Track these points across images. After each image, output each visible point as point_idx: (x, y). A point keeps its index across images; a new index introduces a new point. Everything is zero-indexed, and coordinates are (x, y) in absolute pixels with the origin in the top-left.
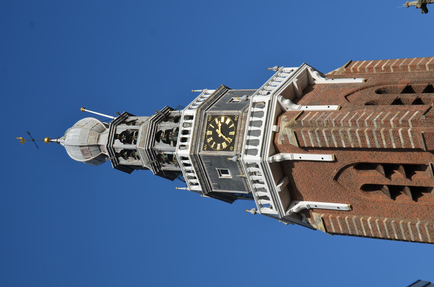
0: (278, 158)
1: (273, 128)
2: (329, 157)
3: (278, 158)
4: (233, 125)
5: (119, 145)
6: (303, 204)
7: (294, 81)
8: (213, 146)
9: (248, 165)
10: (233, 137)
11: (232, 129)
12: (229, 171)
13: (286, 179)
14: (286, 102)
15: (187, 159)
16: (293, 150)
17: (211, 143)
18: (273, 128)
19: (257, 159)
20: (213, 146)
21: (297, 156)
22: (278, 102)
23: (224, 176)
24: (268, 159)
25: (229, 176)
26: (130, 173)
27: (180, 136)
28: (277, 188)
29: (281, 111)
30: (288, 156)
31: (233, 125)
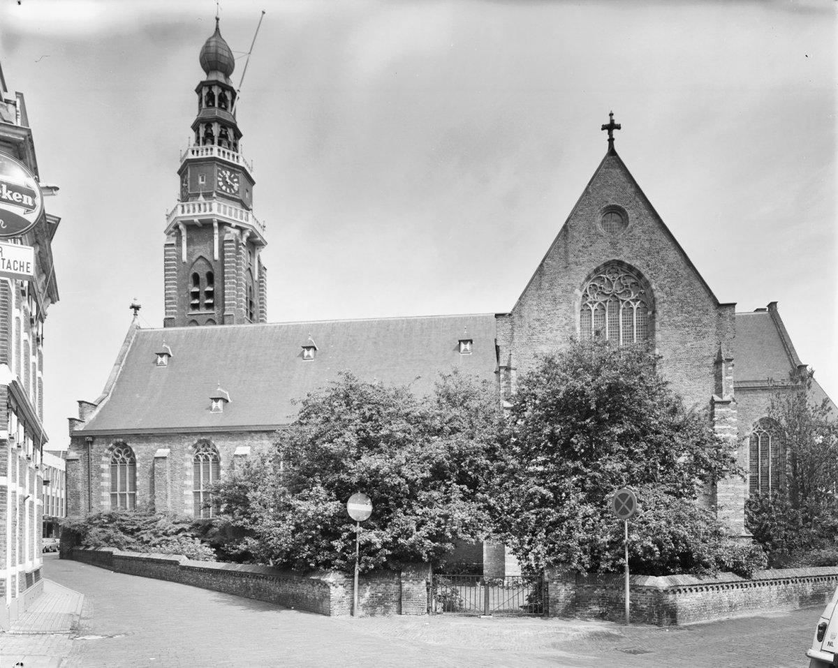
0: (216, 225)
1: (234, 224)
2: (216, 256)
3: (216, 225)
4: (233, 192)
5: (216, 91)
6: (184, 233)
7: (259, 239)
8: (220, 174)
9: (210, 204)
10: (226, 191)
11: (231, 191)
12: (203, 183)
13: (201, 225)
14: (248, 234)
15: (211, 154)
16: (221, 239)
17: (222, 174)
18: (234, 224)
19: (215, 211)
20: (220, 174)
21: (216, 237)
22: (247, 229)
23: (200, 179)
24: (215, 219)
25: (200, 182)
26: (196, 90)
27: (227, 151)
28: (196, 220)
29: (242, 230)
30: (216, 231)
31: (233, 192)
